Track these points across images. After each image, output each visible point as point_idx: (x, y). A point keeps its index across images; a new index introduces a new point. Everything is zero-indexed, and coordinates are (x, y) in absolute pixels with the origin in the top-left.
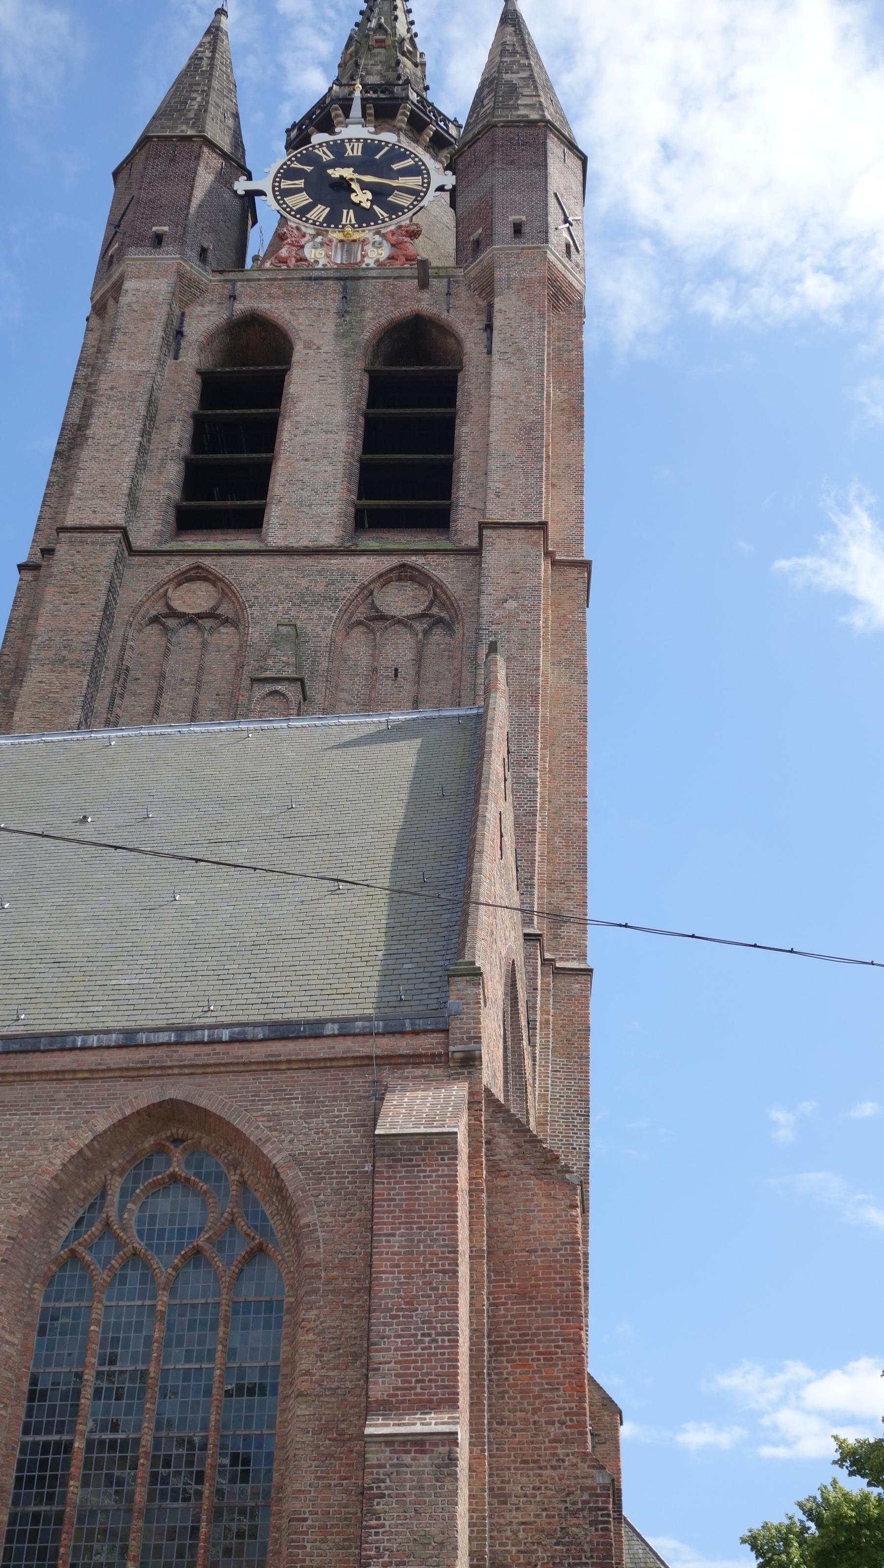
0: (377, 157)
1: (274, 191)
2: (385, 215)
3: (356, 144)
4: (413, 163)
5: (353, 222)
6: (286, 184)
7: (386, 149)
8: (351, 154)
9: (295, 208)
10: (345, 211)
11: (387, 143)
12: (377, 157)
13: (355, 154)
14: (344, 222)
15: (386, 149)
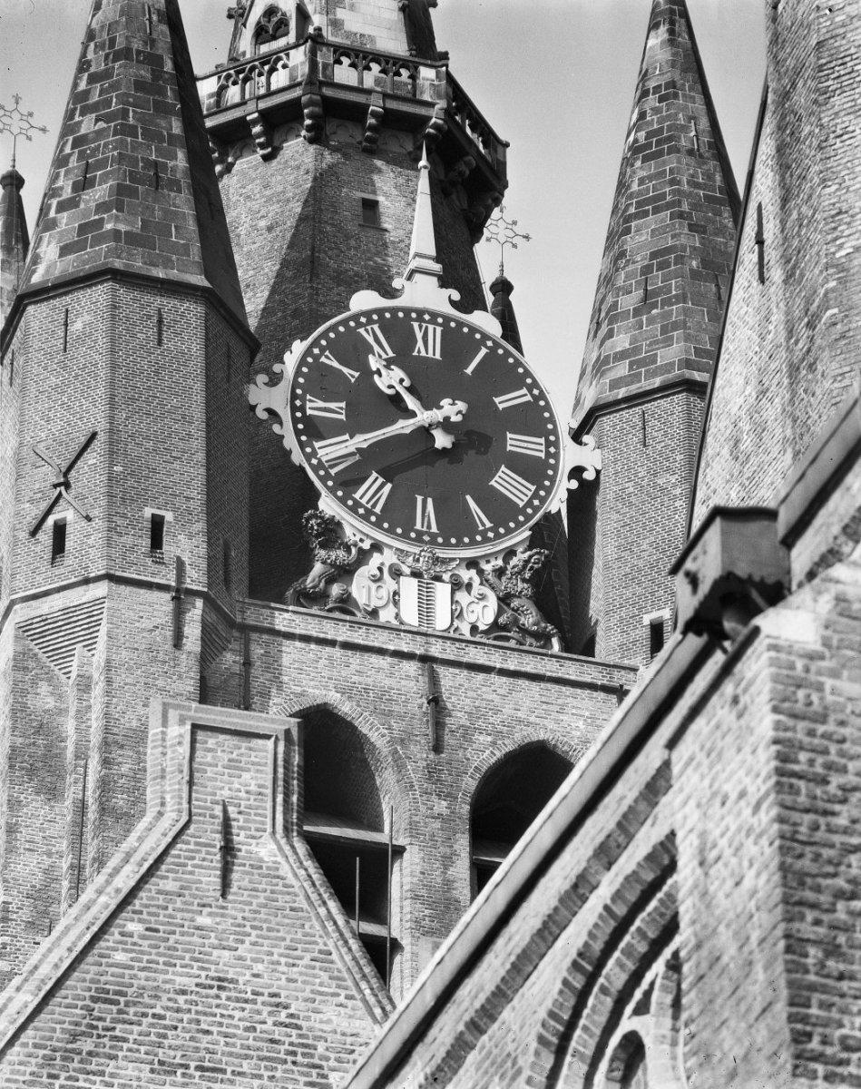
0: (469, 371)
1: (295, 421)
2: (489, 525)
3: (431, 327)
4: (529, 398)
5: (434, 529)
6: (314, 407)
7: (484, 351)
8: (423, 353)
9: (333, 472)
10: (420, 499)
11: (485, 337)
12: (469, 371)
13: (430, 355)
14: (418, 526)
15: (484, 351)
